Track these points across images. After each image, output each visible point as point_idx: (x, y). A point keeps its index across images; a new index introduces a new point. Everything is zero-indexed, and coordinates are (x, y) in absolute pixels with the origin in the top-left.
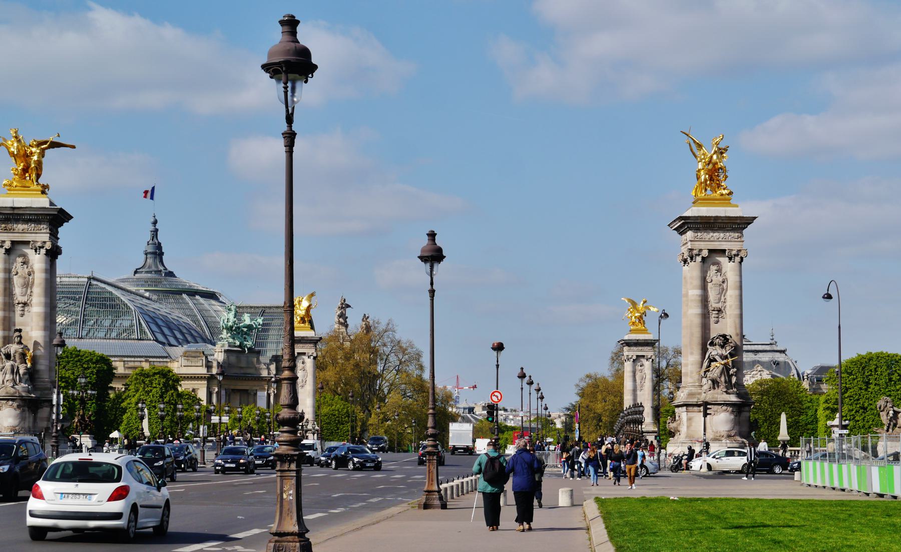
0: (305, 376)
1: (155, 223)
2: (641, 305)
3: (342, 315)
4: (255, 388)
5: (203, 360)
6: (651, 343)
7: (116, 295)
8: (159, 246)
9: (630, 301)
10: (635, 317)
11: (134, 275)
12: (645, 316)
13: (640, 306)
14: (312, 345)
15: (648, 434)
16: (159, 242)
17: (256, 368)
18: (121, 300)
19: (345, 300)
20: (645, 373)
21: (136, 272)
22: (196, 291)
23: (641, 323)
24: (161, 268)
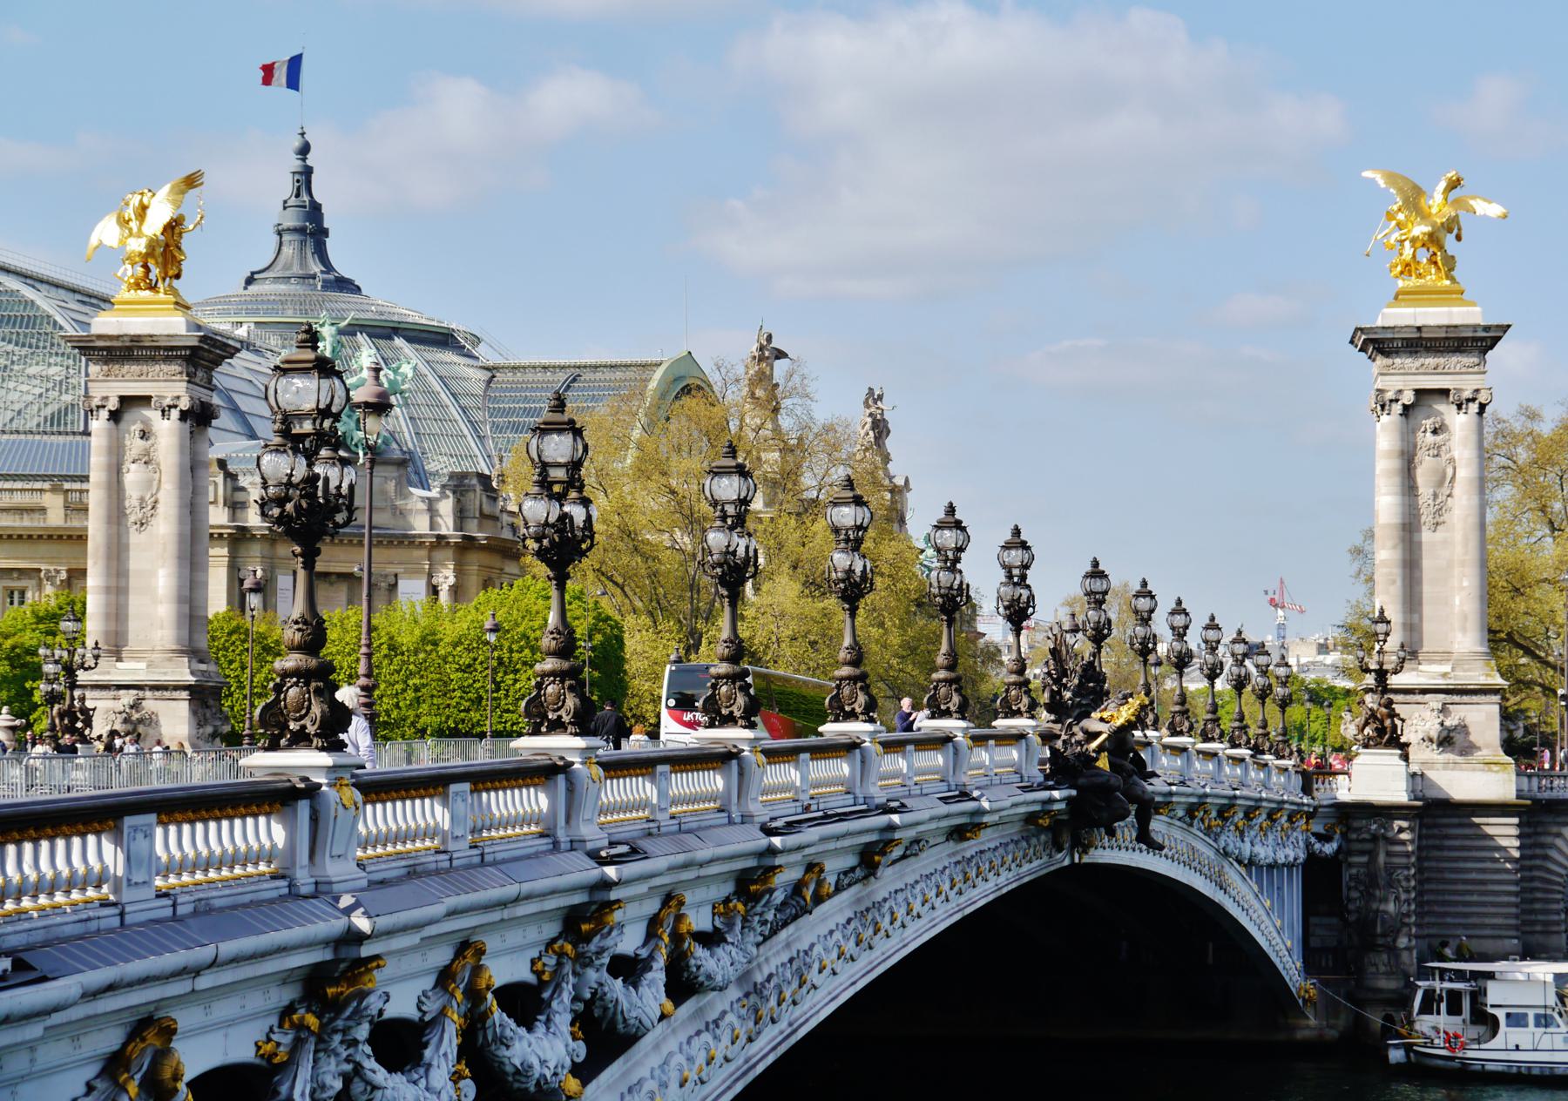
0: (152, 485)
1: (304, 150)
2: (1438, 197)
3: (763, 378)
4: (391, 569)
5: (216, 484)
6: (1475, 339)
7: (44, 311)
8: (314, 211)
9: (1392, 178)
10: (1414, 240)
11: (245, 288)
12: (1458, 238)
13: (1436, 202)
14: (175, 368)
15: (1466, 698)
16: (313, 202)
17: (394, 508)
18: (55, 322)
19: (769, 338)
20: (1452, 460)
21: (250, 281)
22: (396, 325)
23: (1436, 263)
24: (316, 268)
